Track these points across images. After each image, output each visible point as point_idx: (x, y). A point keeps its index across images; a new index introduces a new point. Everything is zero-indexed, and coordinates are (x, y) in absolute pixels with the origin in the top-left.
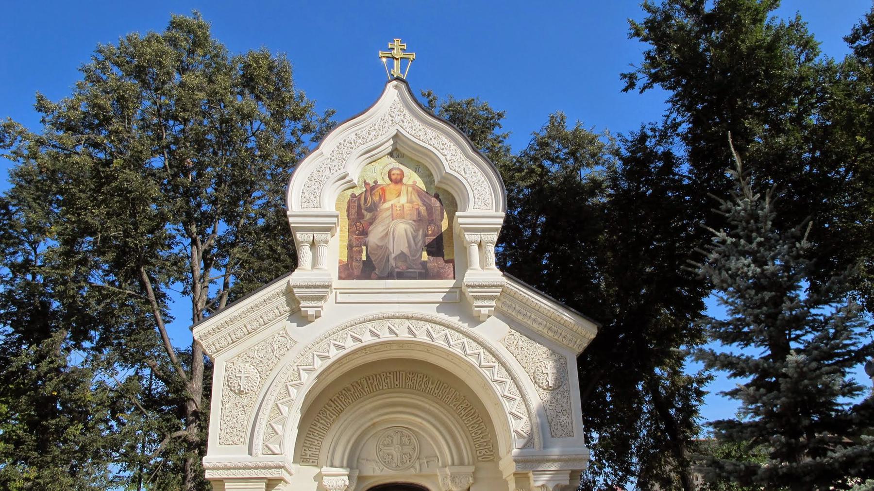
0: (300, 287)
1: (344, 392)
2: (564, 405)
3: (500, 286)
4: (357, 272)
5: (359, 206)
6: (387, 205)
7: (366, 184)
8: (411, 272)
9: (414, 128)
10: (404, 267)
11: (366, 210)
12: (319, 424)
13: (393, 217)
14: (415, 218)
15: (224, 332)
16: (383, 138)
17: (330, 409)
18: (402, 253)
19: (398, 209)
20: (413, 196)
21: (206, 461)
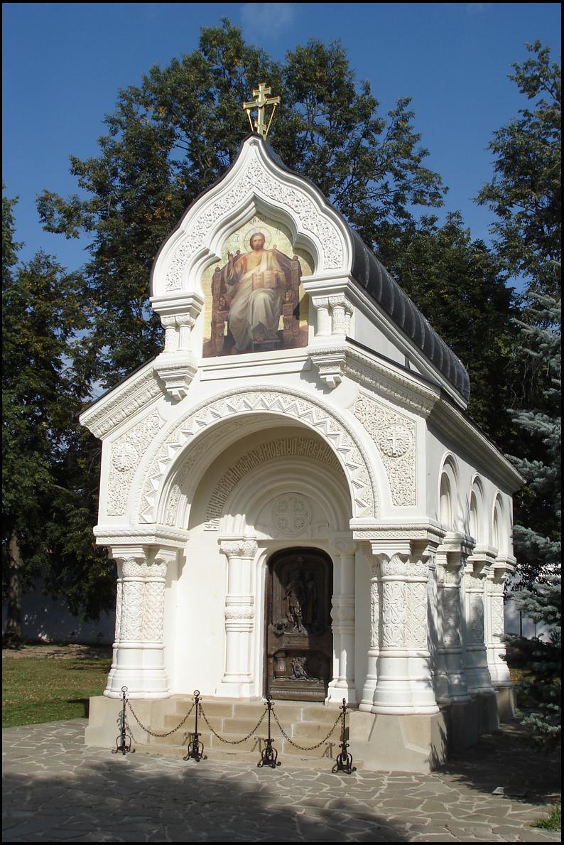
0: (164, 370)
1: (241, 461)
3: (340, 352)
4: (219, 349)
5: (223, 281)
6: (248, 275)
7: (230, 255)
8: (268, 344)
10: (261, 339)
11: (229, 284)
12: (219, 493)
15: (105, 417)
16: (239, 205)
17: (230, 477)
18: (260, 324)
19: (259, 277)
21: (97, 530)
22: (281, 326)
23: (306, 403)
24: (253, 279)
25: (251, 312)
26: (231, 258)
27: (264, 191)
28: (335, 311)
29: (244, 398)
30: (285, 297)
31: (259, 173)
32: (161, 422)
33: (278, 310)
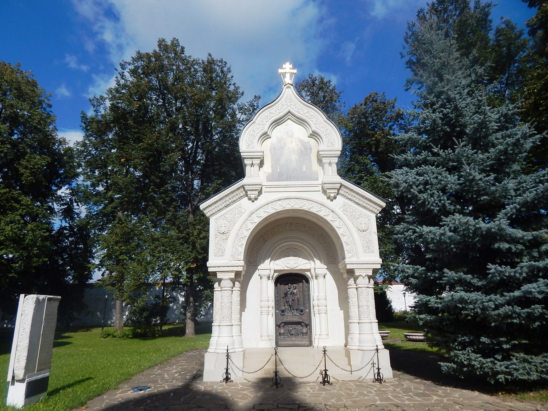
21: (208, 264)
23: (319, 205)
27: (294, 109)
29: (288, 201)
32: (243, 211)
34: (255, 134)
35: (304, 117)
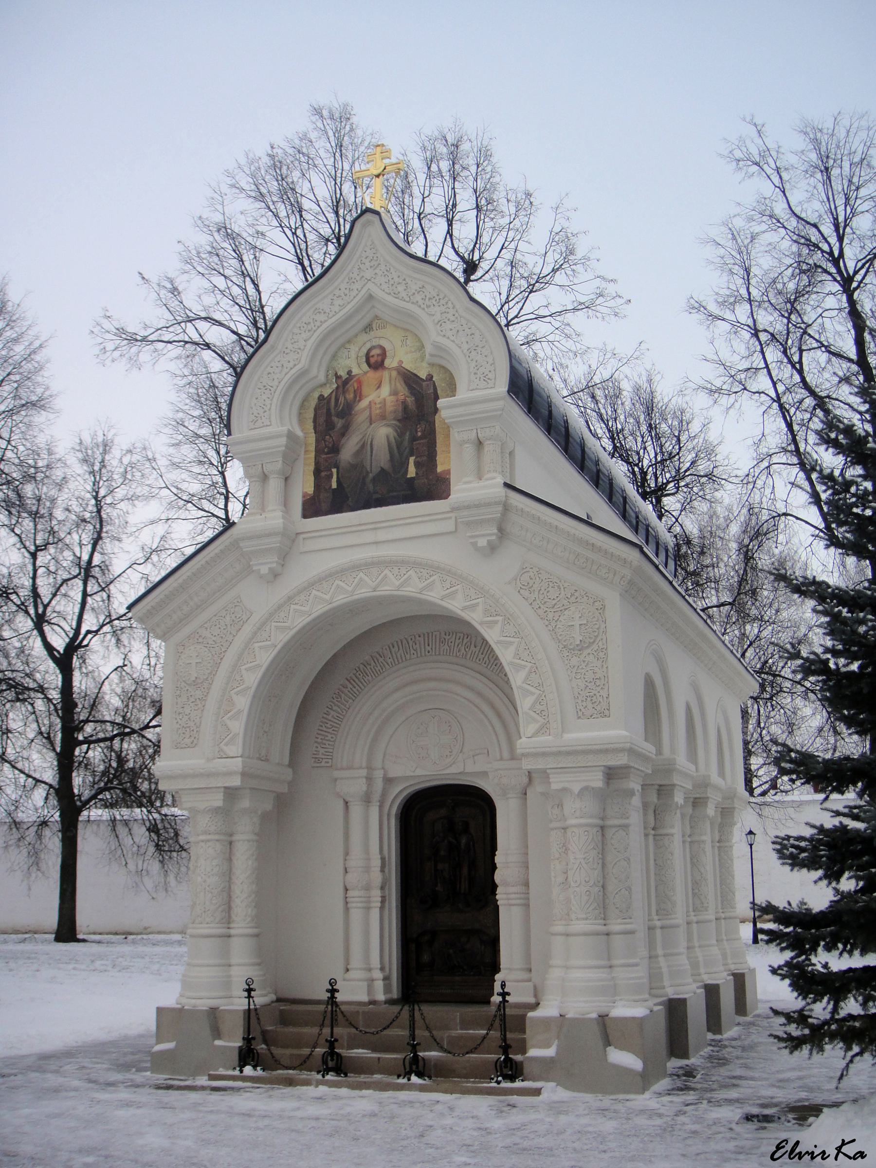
1: (362, 666)
2: (596, 669)
3: (497, 503)
4: (324, 506)
5: (329, 413)
6: (364, 403)
7: (338, 377)
9: (392, 282)
11: (338, 416)
12: (332, 713)
13: (371, 419)
14: (400, 415)
17: (346, 691)
18: (382, 469)
19: (378, 406)
20: (398, 384)
22: (412, 472)
24: (370, 408)
25: (369, 453)
26: (340, 384)
27: (384, 286)
28: (486, 449)
30: (417, 432)
31: (376, 263)
33: (407, 450)
34: (276, 383)
35: (409, 306)
